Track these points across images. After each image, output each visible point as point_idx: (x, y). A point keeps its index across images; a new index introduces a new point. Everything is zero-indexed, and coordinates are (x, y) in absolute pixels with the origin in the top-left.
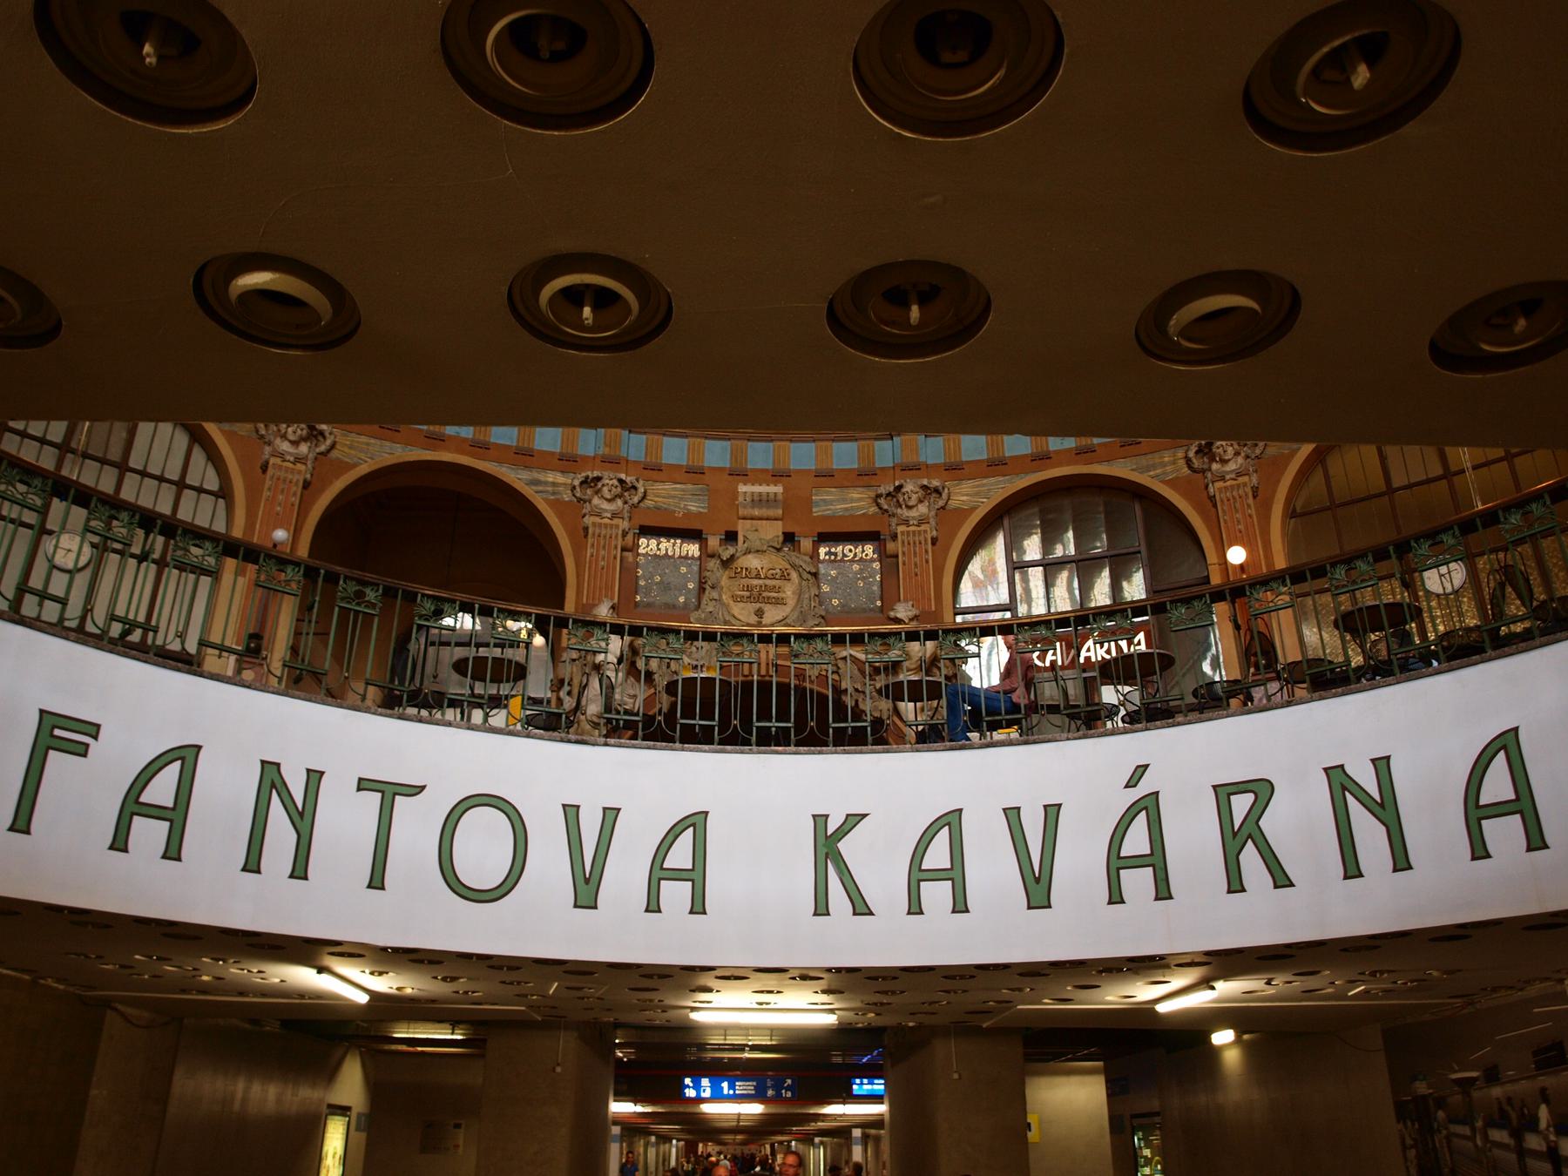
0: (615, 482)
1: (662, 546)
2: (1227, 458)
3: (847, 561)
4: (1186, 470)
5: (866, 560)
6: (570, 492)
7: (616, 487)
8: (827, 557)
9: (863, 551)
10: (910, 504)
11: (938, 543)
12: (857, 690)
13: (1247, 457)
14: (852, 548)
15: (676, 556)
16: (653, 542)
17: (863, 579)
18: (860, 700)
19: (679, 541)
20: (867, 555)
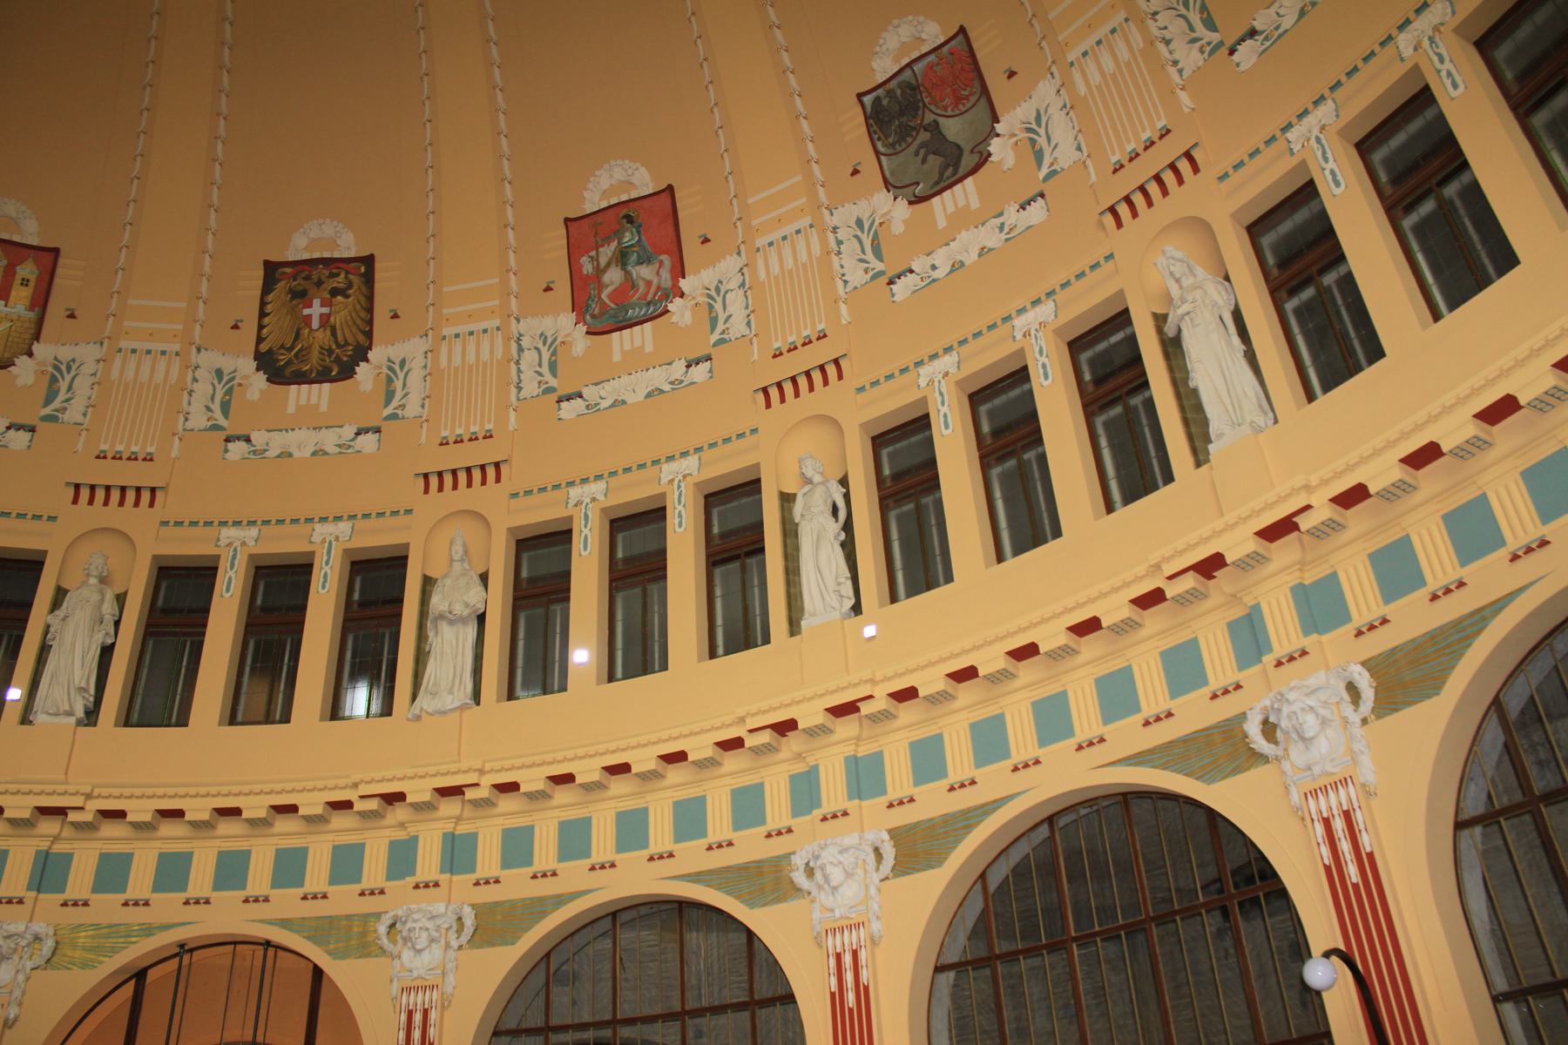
13: (448, 946)
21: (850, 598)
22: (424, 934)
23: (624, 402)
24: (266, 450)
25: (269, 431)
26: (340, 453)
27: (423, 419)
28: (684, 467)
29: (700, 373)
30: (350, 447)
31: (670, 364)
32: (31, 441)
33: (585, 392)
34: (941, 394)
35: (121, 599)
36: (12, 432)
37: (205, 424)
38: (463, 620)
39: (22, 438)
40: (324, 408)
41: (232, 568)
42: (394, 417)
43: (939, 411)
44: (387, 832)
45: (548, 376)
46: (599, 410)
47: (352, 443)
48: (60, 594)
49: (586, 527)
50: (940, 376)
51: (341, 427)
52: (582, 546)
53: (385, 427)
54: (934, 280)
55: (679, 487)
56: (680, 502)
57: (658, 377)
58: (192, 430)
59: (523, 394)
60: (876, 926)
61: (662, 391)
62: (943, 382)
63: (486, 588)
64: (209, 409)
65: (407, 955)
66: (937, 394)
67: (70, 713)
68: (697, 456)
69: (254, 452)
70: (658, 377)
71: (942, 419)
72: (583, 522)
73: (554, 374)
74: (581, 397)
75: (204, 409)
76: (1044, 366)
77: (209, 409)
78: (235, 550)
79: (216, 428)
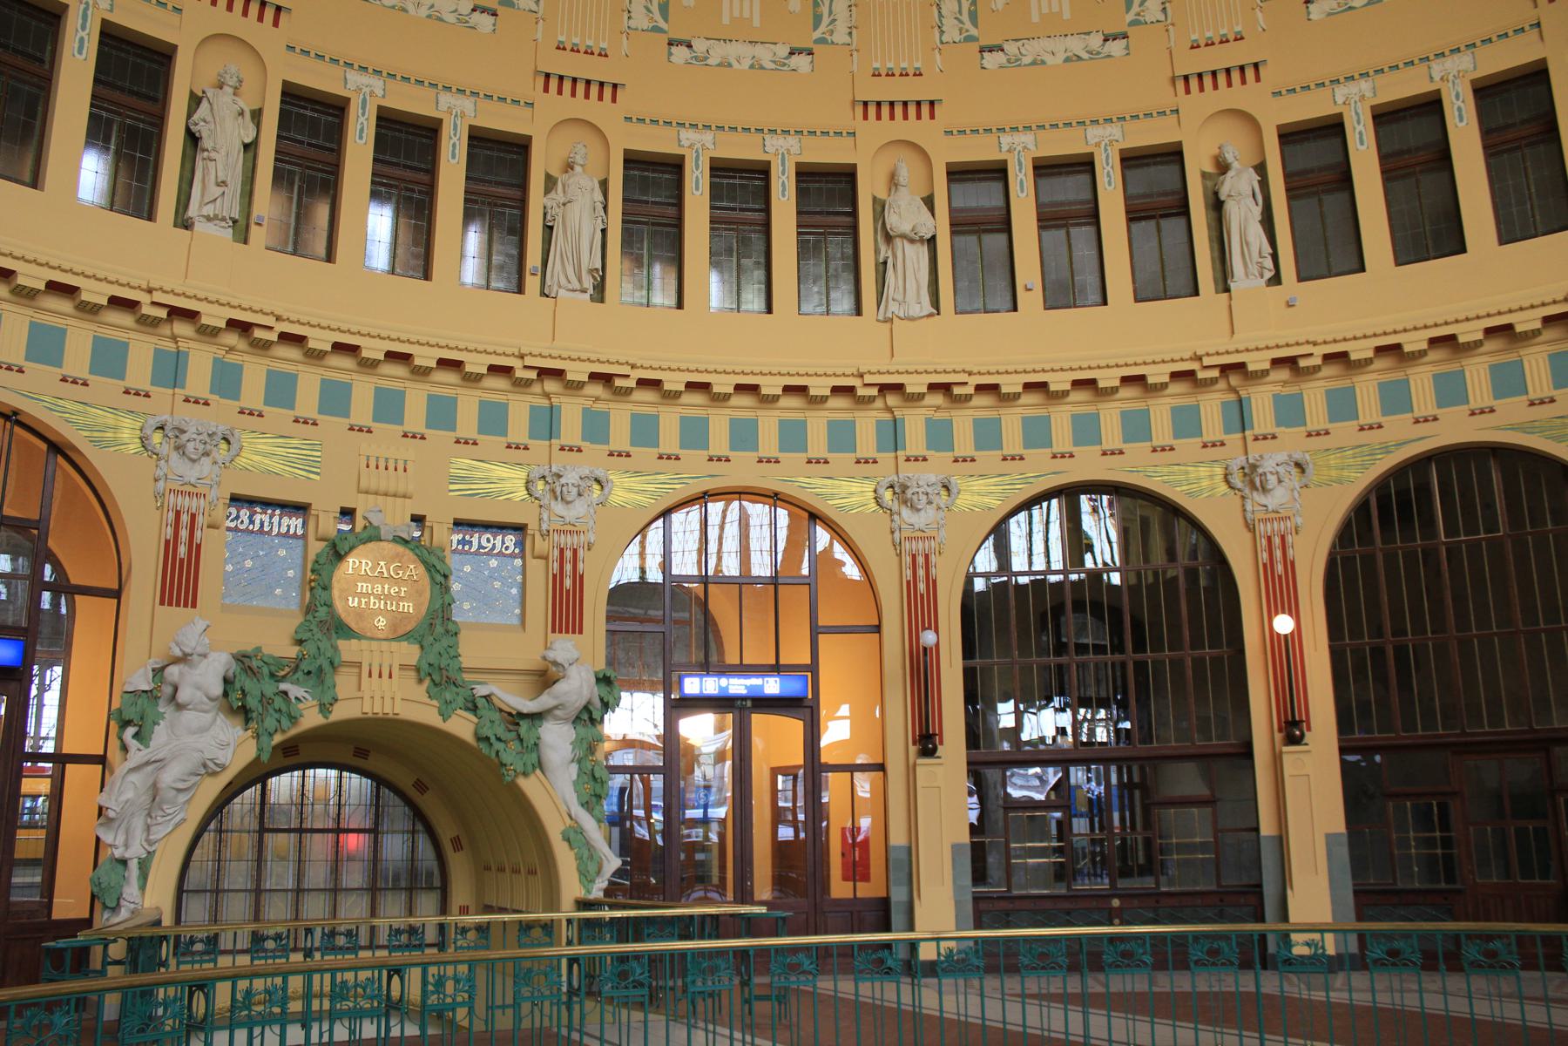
0: (205, 437)
1: (258, 518)
2: (919, 507)
3: (485, 554)
4: (873, 506)
5: (505, 555)
6: (138, 440)
7: (205, 443)
8: (460, 547)
9: (503, 543)
10: (569, 499)
11: (593, 549)
12: (499, 739)
14: (489, 536)
15: (274, 534)
16: (245, 514)
17: (503, 580)
18: (502, 750)
19: (278, 512)
20: (507, 548)
21: (1270, 270)
22: (925, 497)
23: (1043, 62)
24: (706, 58)
25: (707, 39)
26: (776, 69)
27: (854, 47)
28: (1108, 133)
29: (1116, 48)
30: (785, 65)
31: (1088, 33)
32: (494, 25)
33: (1006, 47)
34: (1357, 113)
35: (604, 184)
36: (477, 14)
37: (646, 24)
38: (921, 240)
39: (485, 21)
40: (756, 23)
41: (697, 169)
42: (822, 41)
43: (1354, 128)
44: (874, 413)
45: (968, 25)
46: (1019, 65)
47: (786, 61)
48: (550, 183)
49: (1020, 171)
50: (1357, 99)
51: (776, 44)
52: (1018, 188)
53: (817, 49)
54: (1350, 8)
55: (1106, 150)
56: (1108, 164)
57: (1076, 45)
58: (637, 29)
59: (945, 39)
60: (1299, 520)
61: (1079, 58)
62: (1359, 104)
63: (933, 215)
64: (648, 10)
65: (906, 513)
66: (1353, 114)
67: (584, 291)
68: (1119, 124)
69: (696, 58)
70: (1076, 45)
71: (1357, 136)
72: (1017, 167)
73: (975, 24)
74: (1002, 50)
75: (644, 11)
76: (1459, 109)
77: (648, 10)
78: (697, 151)
79: (656, 29)
